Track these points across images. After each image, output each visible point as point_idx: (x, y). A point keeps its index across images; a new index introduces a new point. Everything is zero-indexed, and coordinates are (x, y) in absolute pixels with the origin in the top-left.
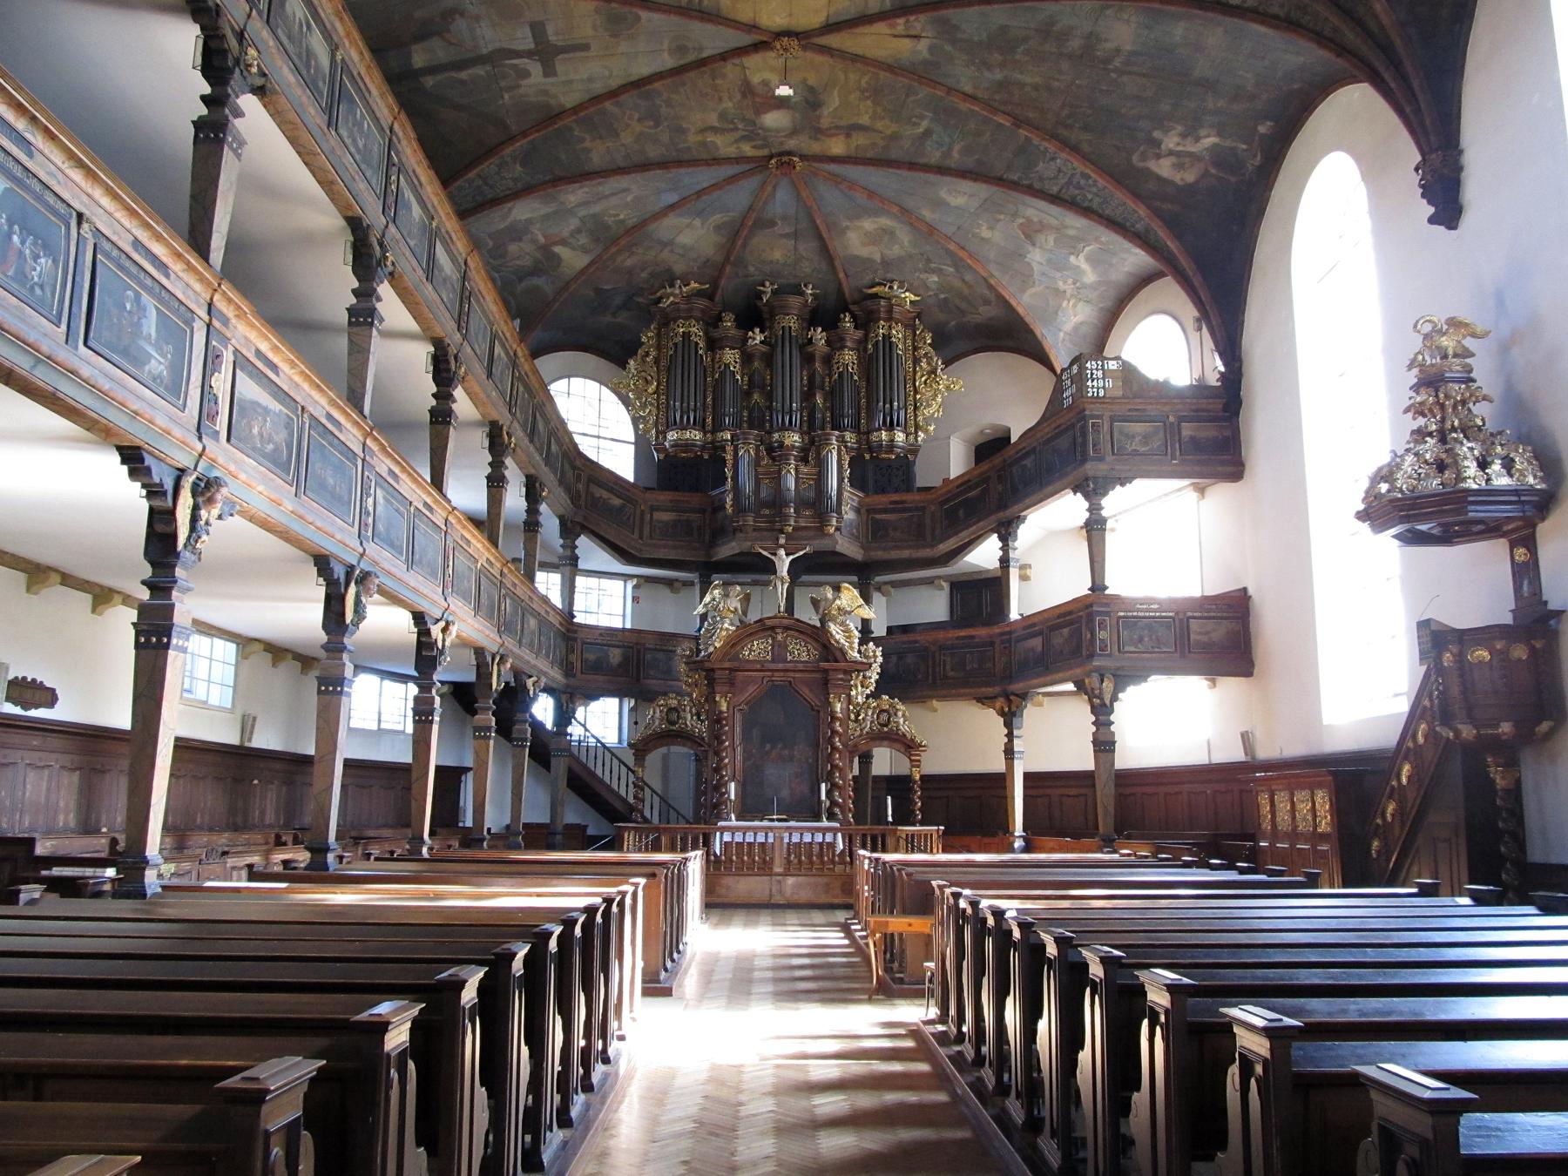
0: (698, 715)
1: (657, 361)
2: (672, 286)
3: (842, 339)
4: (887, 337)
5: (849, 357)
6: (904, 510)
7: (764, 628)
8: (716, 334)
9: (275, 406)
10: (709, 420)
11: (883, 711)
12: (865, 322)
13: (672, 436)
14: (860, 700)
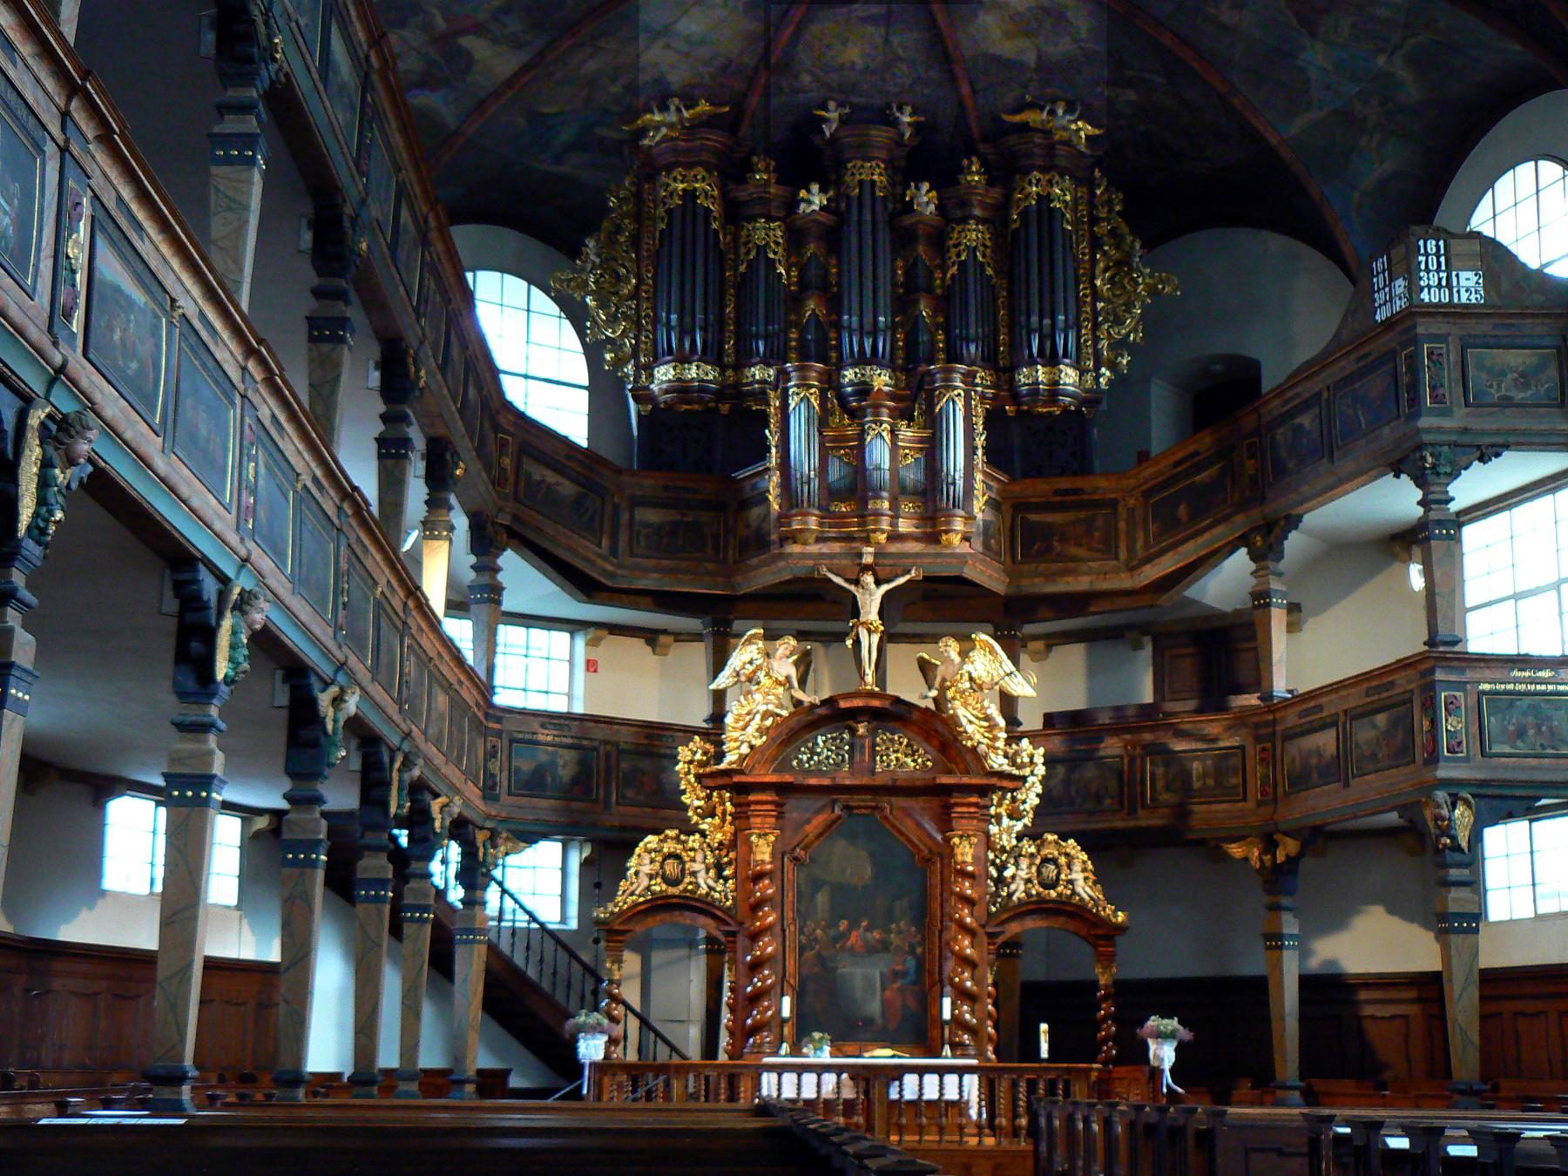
0: (719, 868)
1: (635, 242)
2: (664, 108)
3: (964, 204)
4: (1045, 199)
5: (974, 235)
7: (833, 716)
8: (742, 194)
9: (139, 296)
10: (729, 346)
11: (1045, 860)
12: (1005, 173)
13: (664, 374)
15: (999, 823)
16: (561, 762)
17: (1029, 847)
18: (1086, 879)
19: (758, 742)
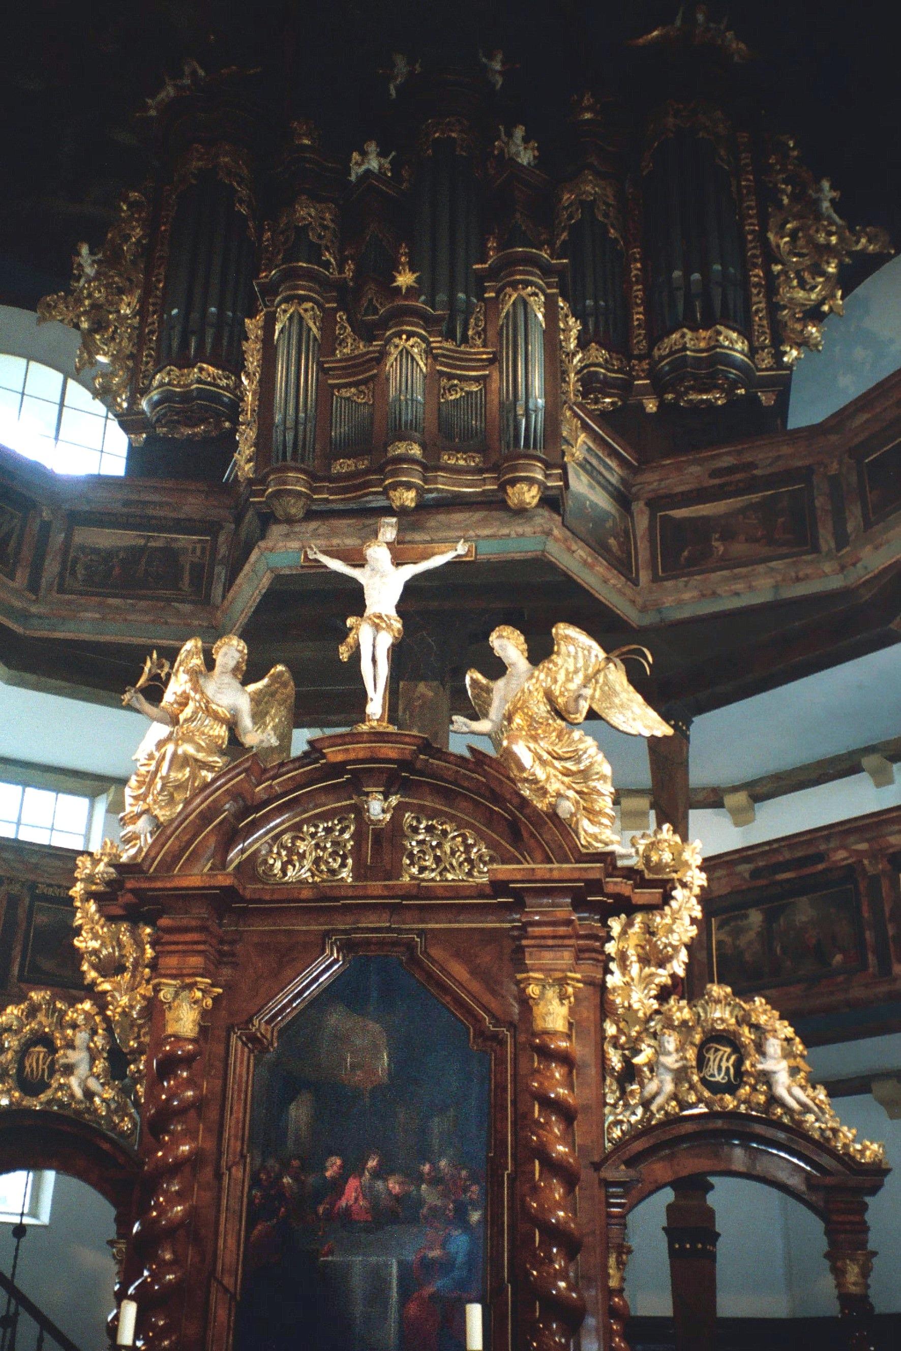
6: (750, 486)
11: (716, 1038)
14: (641, 1000)
15: (624, 968)
17: (680, 1011)
18: (794, 1071)
19: (163, 814)
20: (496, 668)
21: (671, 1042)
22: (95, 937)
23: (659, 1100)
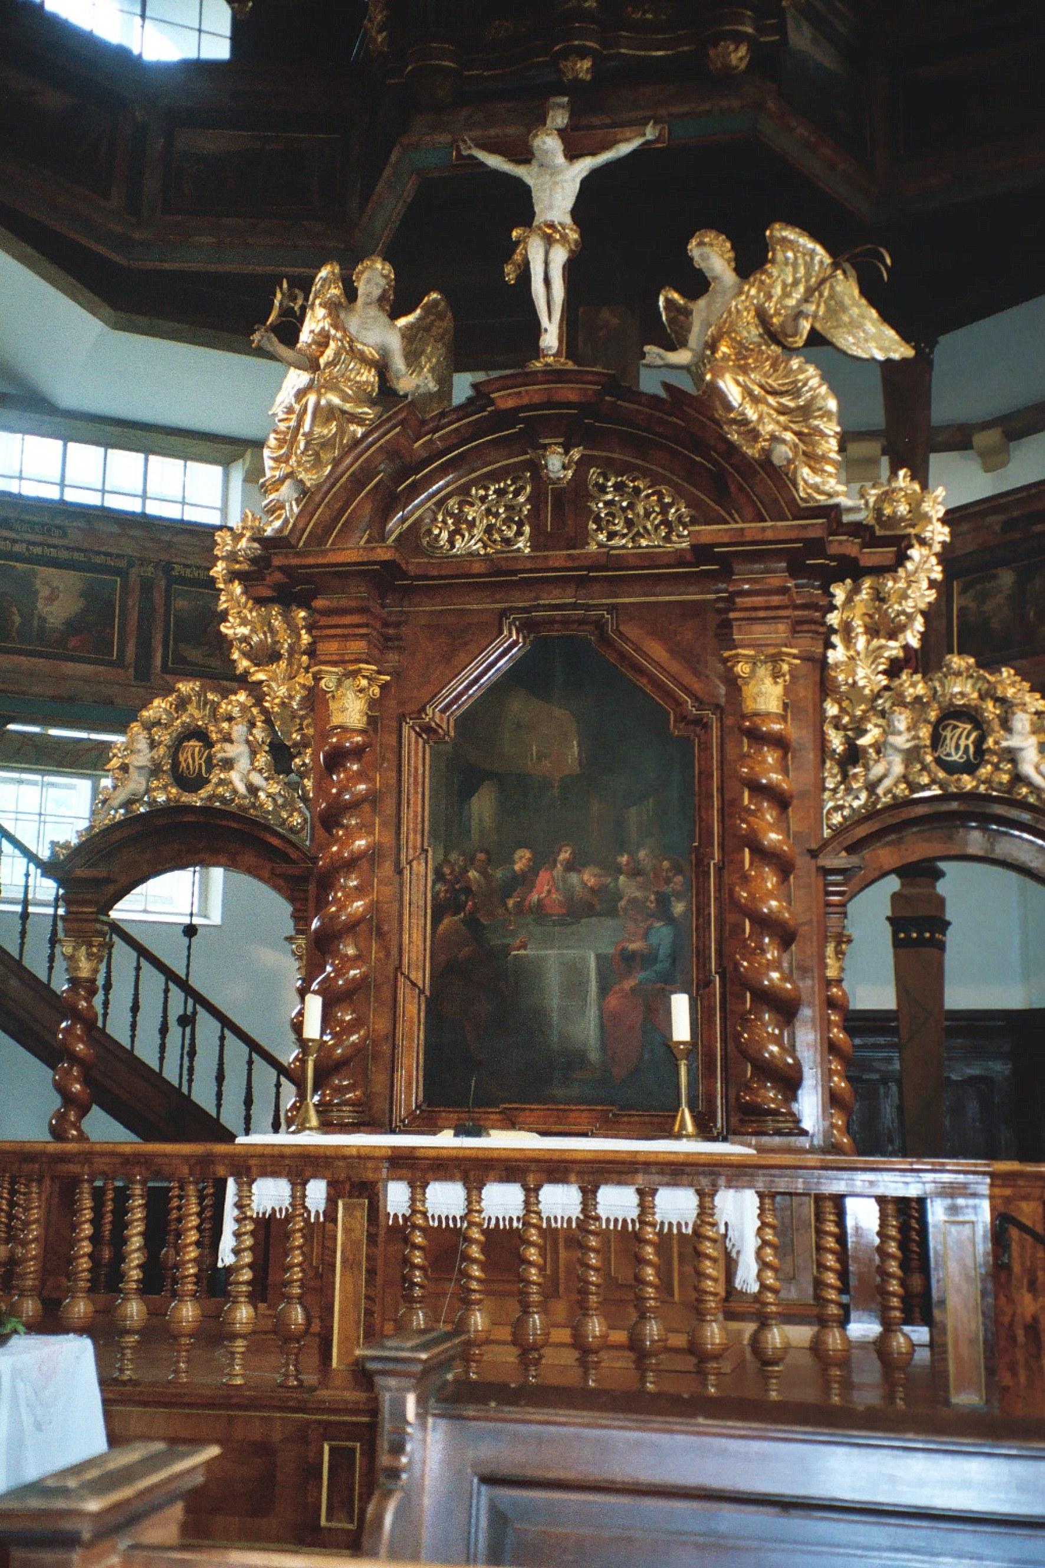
11: (953, 714)
14: (867, 677)
15: (849, 640)
16: (45, 592)
17: (914, 686)
19: (309, 478)
20: (697, 284)
21: (902, 720)
22: (244, 622)
23: (887, 783)
